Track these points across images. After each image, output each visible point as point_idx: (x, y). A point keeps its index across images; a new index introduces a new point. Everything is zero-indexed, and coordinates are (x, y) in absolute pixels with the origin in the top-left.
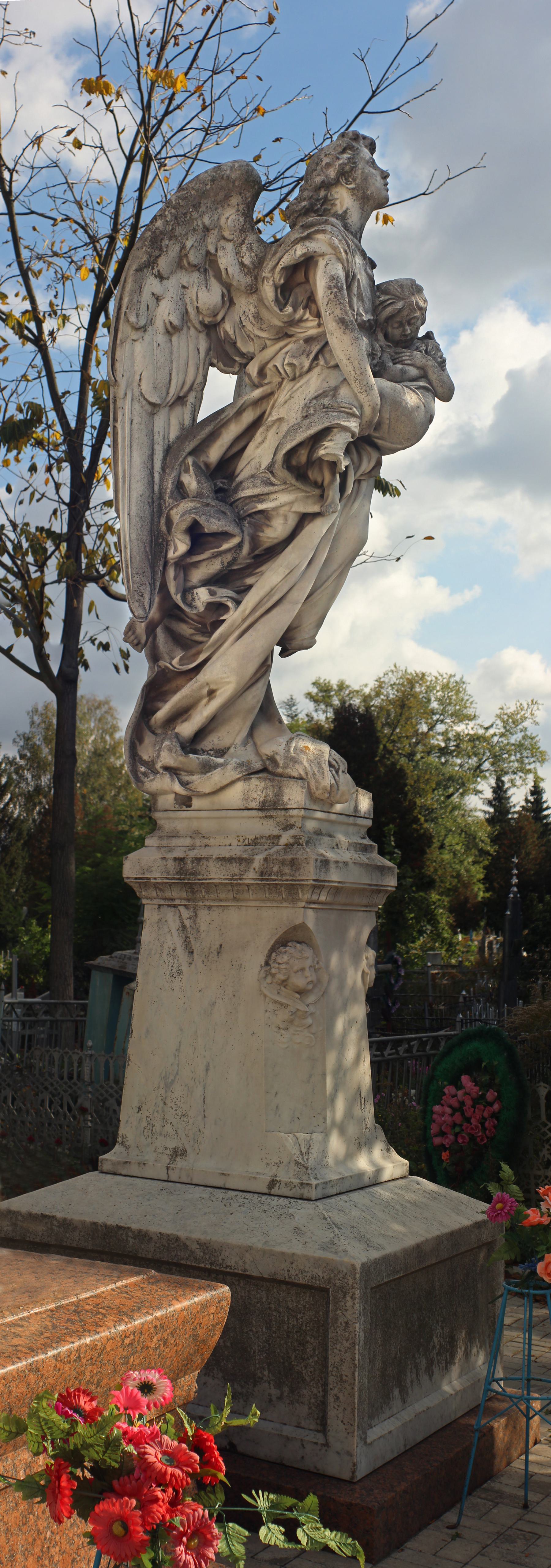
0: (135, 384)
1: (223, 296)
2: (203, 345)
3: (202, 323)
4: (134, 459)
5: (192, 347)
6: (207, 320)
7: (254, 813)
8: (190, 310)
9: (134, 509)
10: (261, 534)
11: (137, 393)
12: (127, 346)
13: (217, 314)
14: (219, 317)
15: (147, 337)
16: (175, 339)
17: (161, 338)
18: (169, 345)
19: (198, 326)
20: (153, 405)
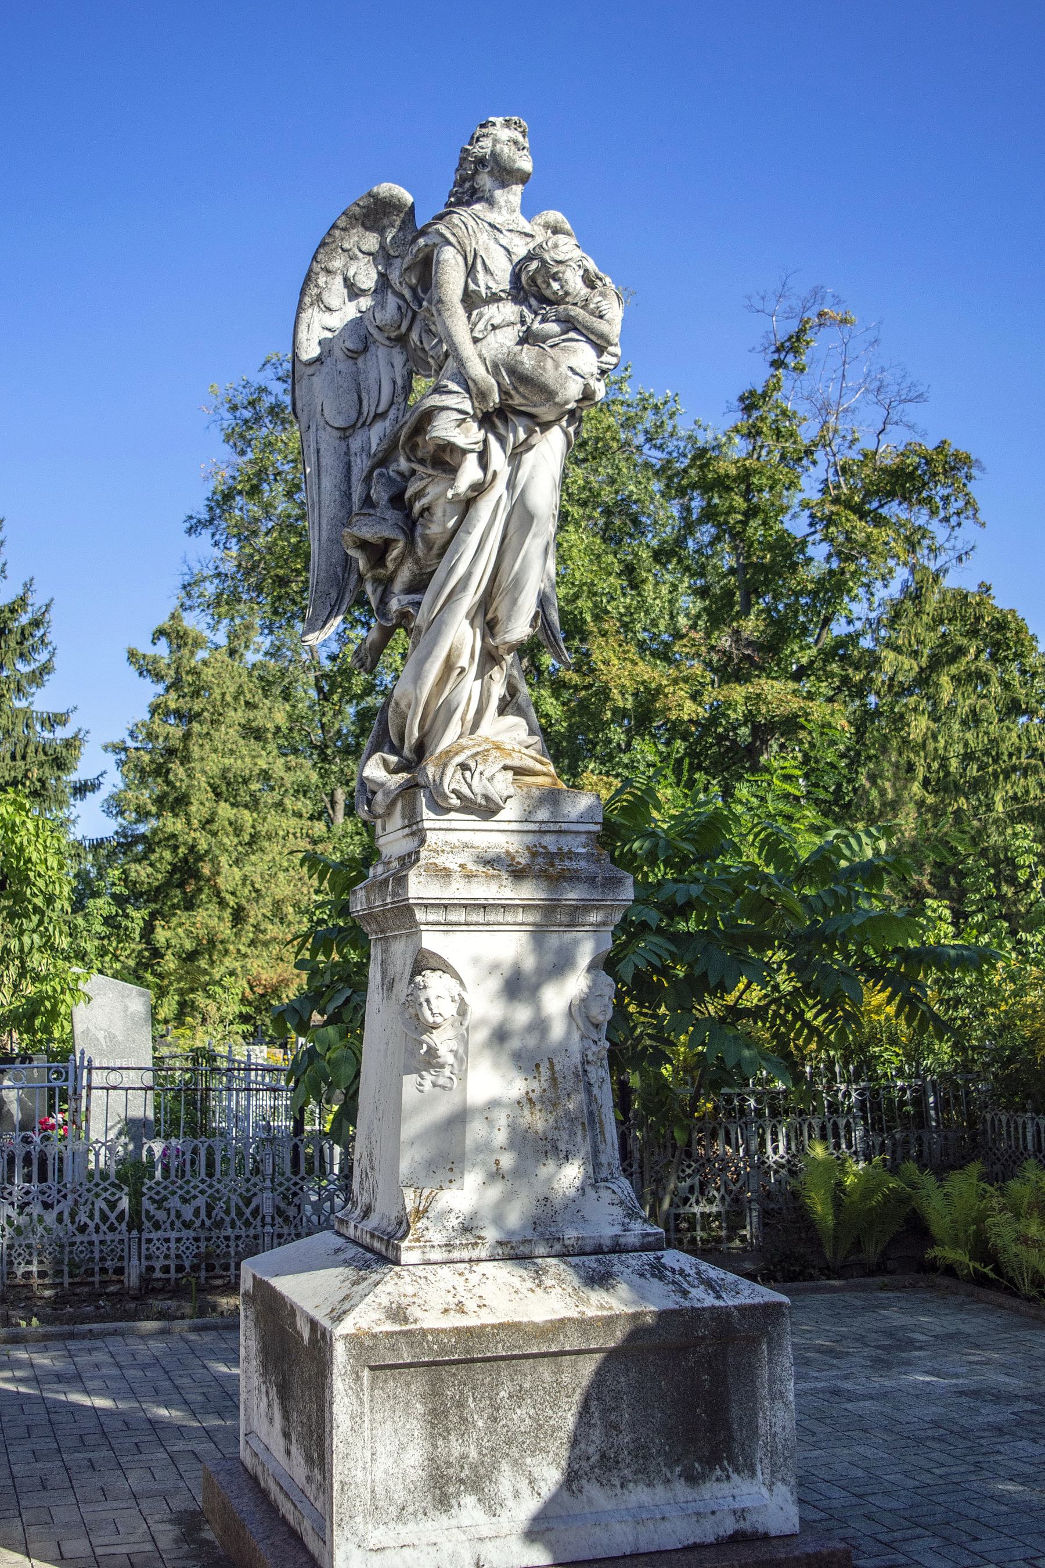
0: (318, 415)
1: (399, 308)
2: (398, 359)
3: (389, 338)
4: (323, 486)
5: (382, 363)
6: (393, 335)
7: (407, 831)
8: (372, 331)
9: (324, 533)
10: (428, 532)
11: (322, 423)
12: (305, 382)
13: (399, 327)
14: (403, 329)
15: (325, 369)
16: (360, 361)
17: (345, 366)
18: (354, 369)
19: (387, 343)
20: (344, 429)
